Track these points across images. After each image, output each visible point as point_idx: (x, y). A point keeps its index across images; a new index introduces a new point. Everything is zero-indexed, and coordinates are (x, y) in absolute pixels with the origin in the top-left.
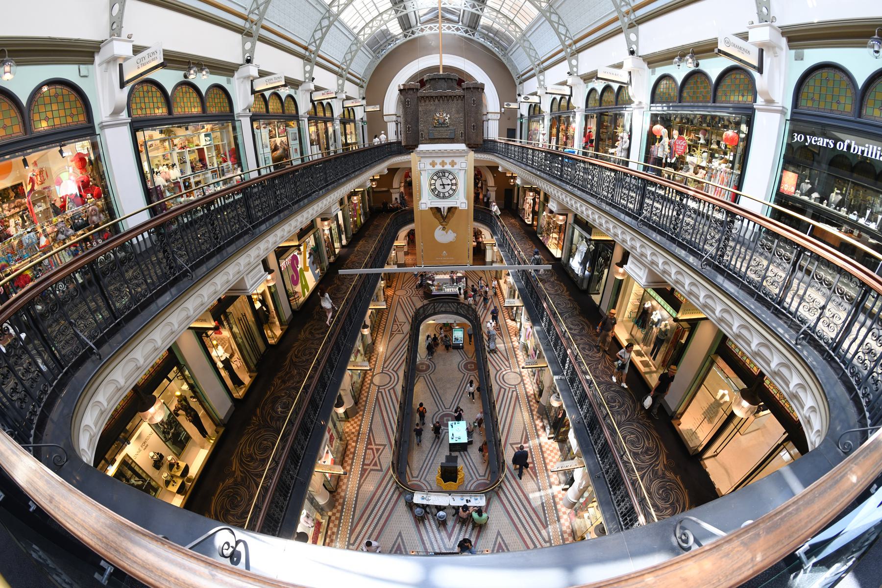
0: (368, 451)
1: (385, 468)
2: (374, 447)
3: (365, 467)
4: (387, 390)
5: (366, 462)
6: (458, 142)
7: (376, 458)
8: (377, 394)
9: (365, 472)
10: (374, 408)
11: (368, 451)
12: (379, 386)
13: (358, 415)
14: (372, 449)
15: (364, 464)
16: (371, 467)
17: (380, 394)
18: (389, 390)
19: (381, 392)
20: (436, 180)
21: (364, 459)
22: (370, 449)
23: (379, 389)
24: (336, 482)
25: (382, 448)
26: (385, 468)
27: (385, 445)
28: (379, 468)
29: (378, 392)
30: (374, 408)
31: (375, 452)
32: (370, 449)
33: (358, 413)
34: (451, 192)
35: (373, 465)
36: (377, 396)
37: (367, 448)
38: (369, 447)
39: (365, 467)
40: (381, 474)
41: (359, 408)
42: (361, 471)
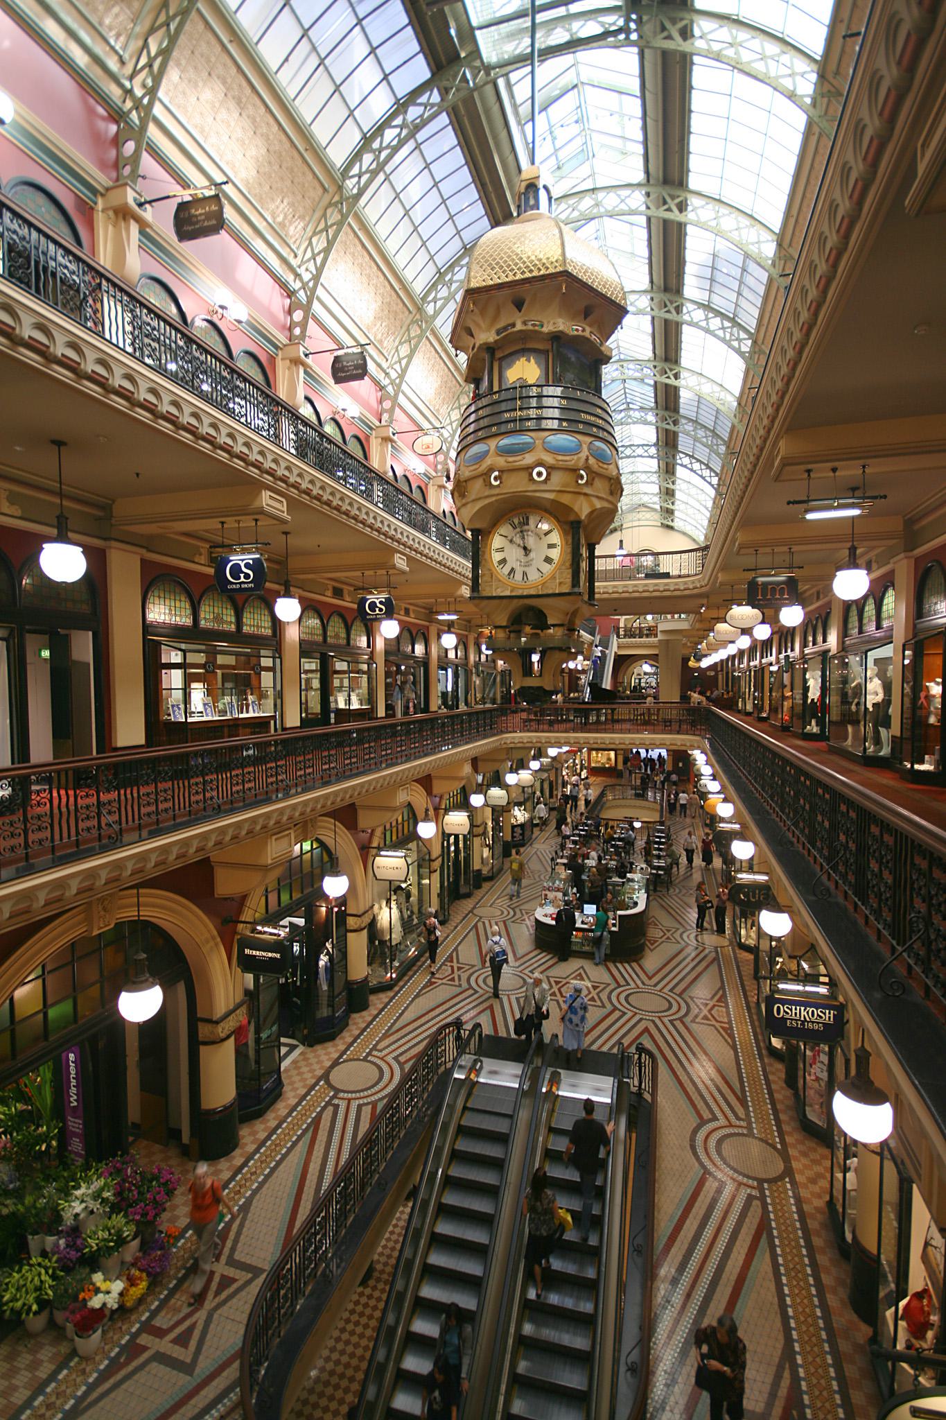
3: (144, 1339)
4: (354, 1104)
5: (159, 1322)
8: (324, 1108)
10: (295, 1144)
12: (337, 1091)
16: (165, 1345)
17: (331, 1108)
18: (360, 1107)
19: (337, 1107)
23: (334, 1097)
29: (328, 1103)
30: (295, 1144)
36: (320, 1115)
39: (144, 1339)
40: (183, 1382)
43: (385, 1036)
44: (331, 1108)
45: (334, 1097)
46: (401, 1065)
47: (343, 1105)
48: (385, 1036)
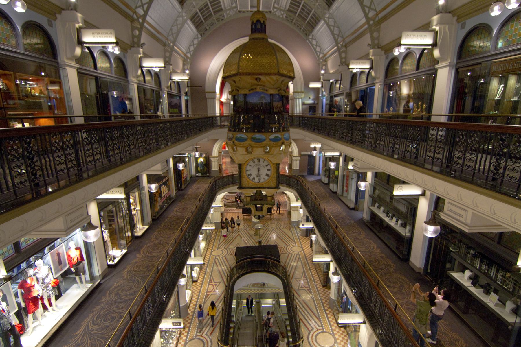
0: (210, 286)
2: (213, 283)
5: (208, 291)
12: (216, 256)
14: (212, 285)
18: (222, 257)
19: (217, 259)
21: (207, 290)
24: (190, 298)
25: (218, 283)
29: (215, 258)
31: (214, 286)
37: (209, 284)
39: (208, 293)
43: (219, 245)
46: (226, 249)
47: (218, 258)
48: (219, 245)
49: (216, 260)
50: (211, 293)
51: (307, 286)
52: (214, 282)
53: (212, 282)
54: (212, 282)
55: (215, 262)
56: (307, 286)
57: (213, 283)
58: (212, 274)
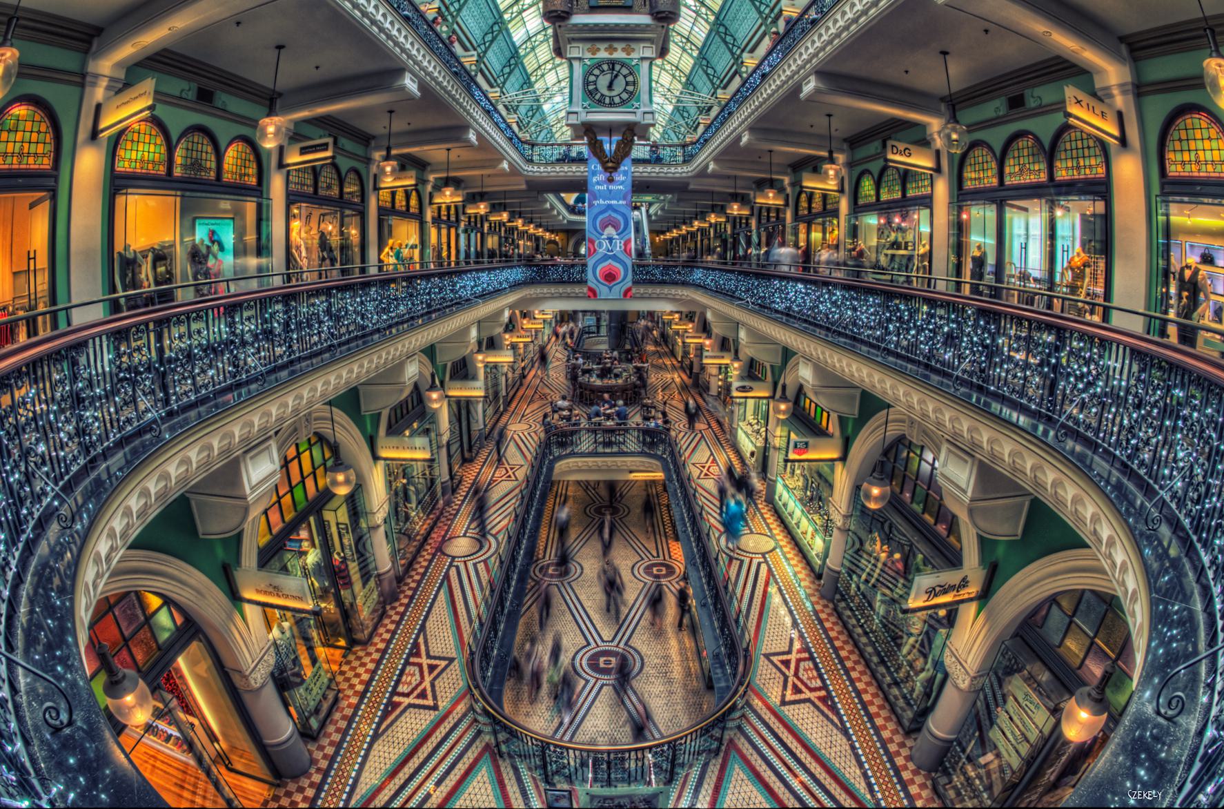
1: (443, 704)
2: (424, 661)
3: (396, 699)
4: (470, 565)
5: (401, 689)
6: (638, 13)
7: (427, 684)
8: (448, 570)
9: (394, 709)
11: (408, 669)
12: (453, 558)
13: (397, 604)
15: (394, 692)
16: (411, 700)
17: (453, 569)
18: (475, 565)
19: (457, 567)
20: (597, 76)
21: (398, 682)
22: (414, 664)
26: (443, 704)
27: (451, 660)
28: (430, 702)
29: (451, 565)
32: (414, 664)
33: (397, 599)
34: (625, 96)
35: (418, 697)
38: (412, 660)
39: (396, 699)
41: (403, 592)
42: (386, 706)
44: (453, 569)
45: (453, 561)
49: (453, 572)
50: (406, 701)
51: (819, 683)
52: (429, 656)
53: (418, 655)
54: (418, 655)
55: (447, 577)
56: (819, 683)
57: (424, 661)
58: (427, 624)
